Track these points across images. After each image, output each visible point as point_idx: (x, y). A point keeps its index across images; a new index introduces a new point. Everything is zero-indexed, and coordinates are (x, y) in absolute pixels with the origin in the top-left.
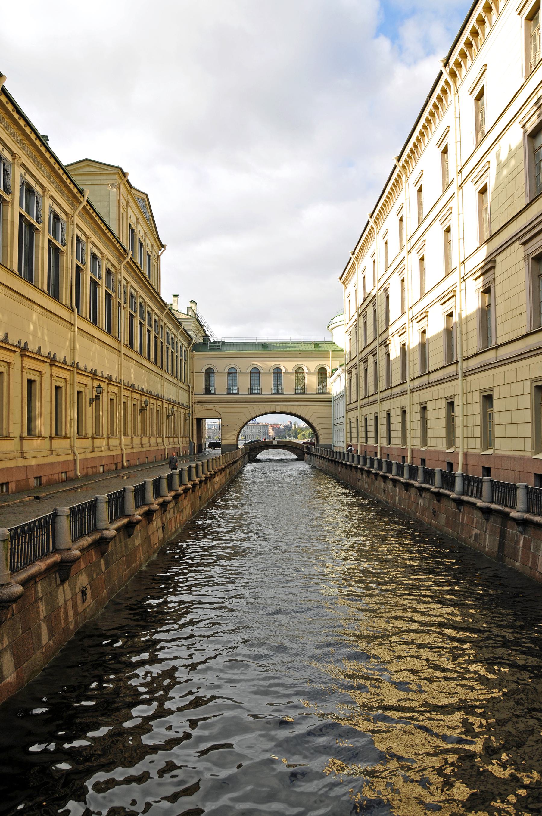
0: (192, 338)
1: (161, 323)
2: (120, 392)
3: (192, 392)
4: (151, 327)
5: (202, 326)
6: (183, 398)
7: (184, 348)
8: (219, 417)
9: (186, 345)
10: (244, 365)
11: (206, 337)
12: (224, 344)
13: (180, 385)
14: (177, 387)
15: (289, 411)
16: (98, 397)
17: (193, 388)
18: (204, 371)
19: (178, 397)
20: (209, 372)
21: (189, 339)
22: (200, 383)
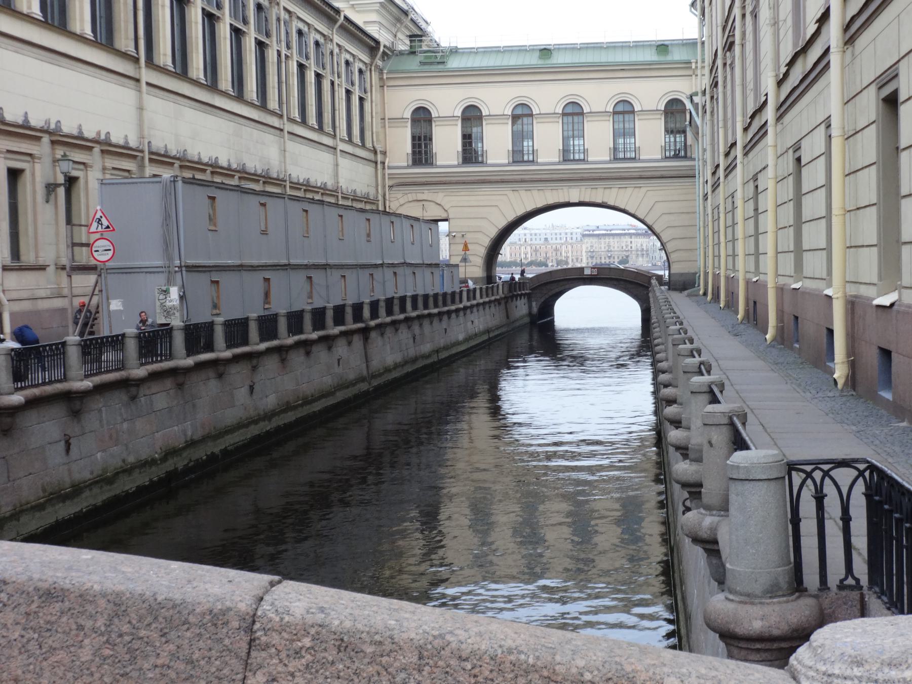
0: (377, 42)
1: (274, 13)
2: (142, 167)
3: (383, 163)
4: (245, 22)
5: (406, 13)
6: (354, 177)
7: (357, 65)
8: (444, 216)
9: (366, 59)
10: (496, 99)
11: (418, 36)
12: (454, 51)
13: (342, 146)
14: (335, 154)
15: (599, 201)
16: (71, 181)
17: (384, 153)
18: (408, 114)
19: (336, 175)
20: (422, 117)
21: (372, 46)
22: (400, 144)
